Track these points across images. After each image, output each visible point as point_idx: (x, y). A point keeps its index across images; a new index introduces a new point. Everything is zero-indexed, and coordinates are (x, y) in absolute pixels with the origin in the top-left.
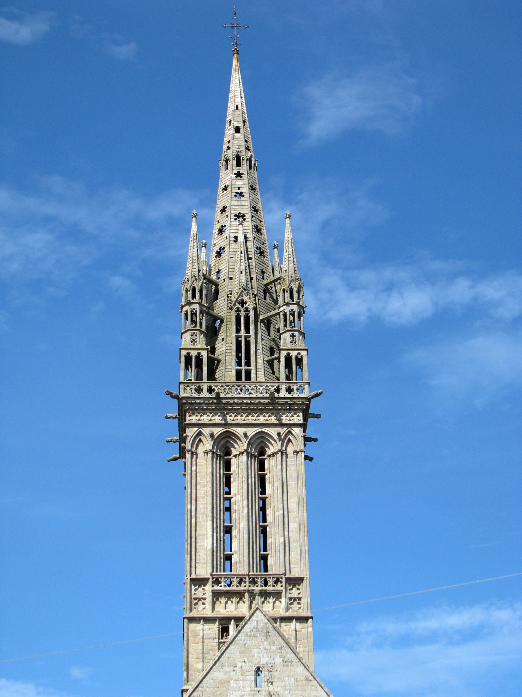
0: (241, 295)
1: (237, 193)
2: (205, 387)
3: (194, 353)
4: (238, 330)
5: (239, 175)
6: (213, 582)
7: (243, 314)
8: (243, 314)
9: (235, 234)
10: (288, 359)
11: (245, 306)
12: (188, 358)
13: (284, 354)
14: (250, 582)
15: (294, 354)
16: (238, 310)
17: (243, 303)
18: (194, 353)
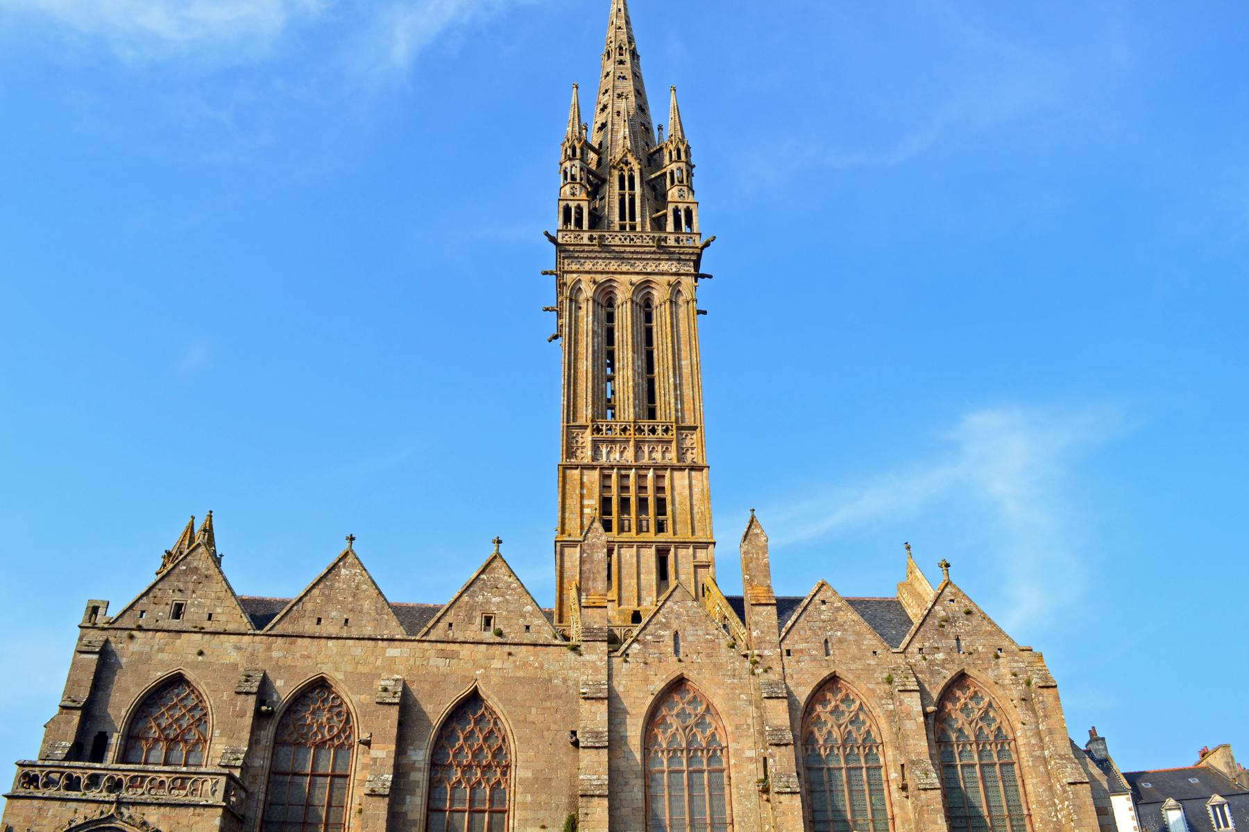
0: (625, 156)
1: (620, 77)
2: (586, 236)
3: (573, 205)
4: (622, 187)
5: (621, 62)
6: (593, 430)
7: (626, 174)
8: (626, 174)
9: (618, 110)
10: (676, 211)
11: (629, 166)
12: (567, 210)
13: (671, 207)
14: (635, 430)
15: (682, 207)
16: (622, 169)
17: (627, 163)
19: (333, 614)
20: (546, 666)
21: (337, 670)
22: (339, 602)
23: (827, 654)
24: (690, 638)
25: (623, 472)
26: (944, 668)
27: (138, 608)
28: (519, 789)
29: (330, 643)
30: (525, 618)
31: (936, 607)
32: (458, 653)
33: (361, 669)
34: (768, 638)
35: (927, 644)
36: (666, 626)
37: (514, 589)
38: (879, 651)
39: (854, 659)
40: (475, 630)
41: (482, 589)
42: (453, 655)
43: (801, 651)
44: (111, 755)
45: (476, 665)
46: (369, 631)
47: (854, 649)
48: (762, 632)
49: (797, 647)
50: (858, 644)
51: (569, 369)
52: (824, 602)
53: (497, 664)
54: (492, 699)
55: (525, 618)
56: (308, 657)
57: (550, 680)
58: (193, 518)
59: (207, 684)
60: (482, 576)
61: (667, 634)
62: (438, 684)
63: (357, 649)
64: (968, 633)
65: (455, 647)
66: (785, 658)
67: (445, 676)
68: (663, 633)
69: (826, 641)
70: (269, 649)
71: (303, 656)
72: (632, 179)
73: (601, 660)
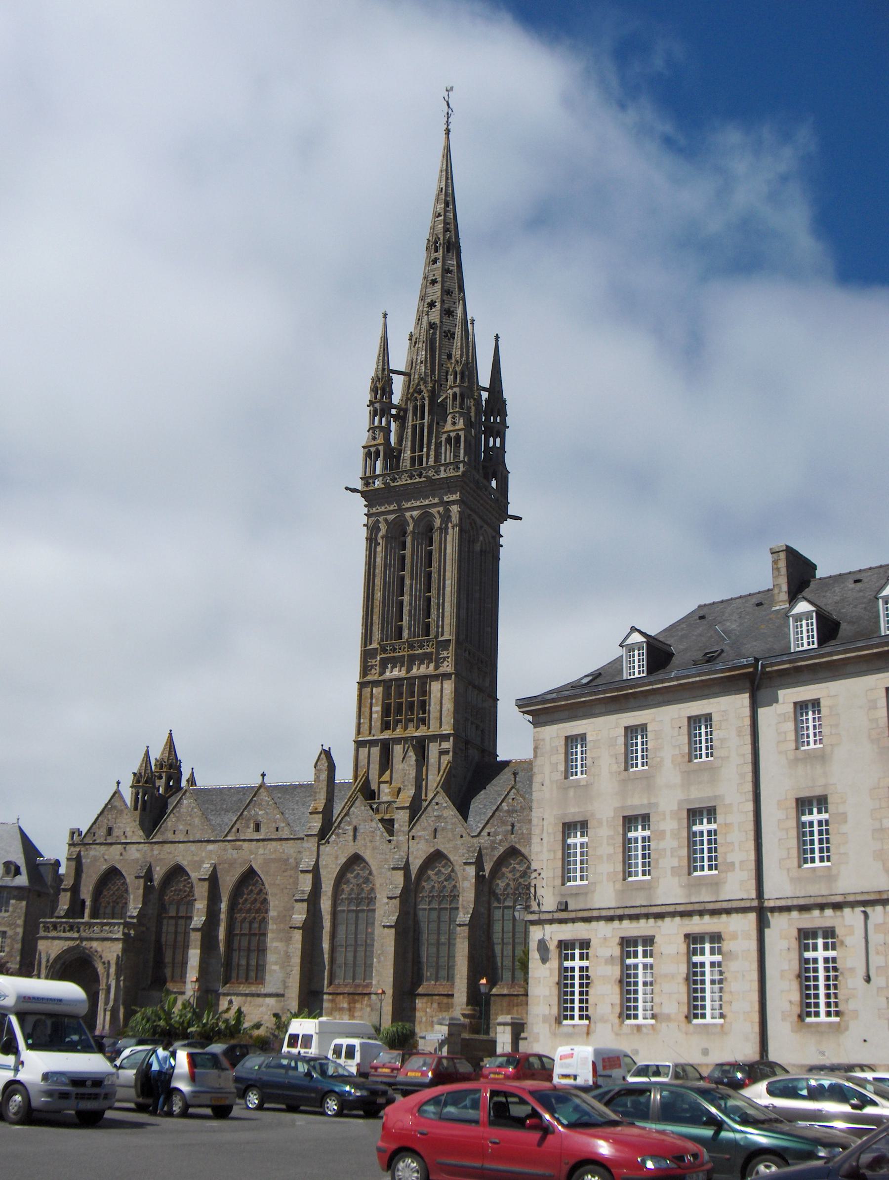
0: (418, 384)
13: (444, 436)
14: (408, 648)
18: (373, 449)
19: (181, 827)
20: (286, 851)
21: (184, 860)
22: (184, 820)
23: (435, 837)
24: (362, 831)
25: (399, 682)
26: (500, 845)
27: (92, 831)
28: (270, 922)
29: (180, 845)
30: (275, 822)
31: (503, 804)
32: (241, 846)
33: (196, 858)
34: (402, 829)
35: (493, 830)
36: (349, 823)
37: (271, 805)
38: (464, 835)
39: (450, 840)
40: (250, 833)
41: (254, 807)
42: (239, 848)
43: (420, 837)
44: (87, 912)
45: (251, 853)
46: (198, 837)
47: (450, 835)
48: (400, 825)
49: (420, 834)
50: (453, 831)
51: (368, 601)
52: (437, 804)
53: (261, 851)
54: (259, 872)
55: (275, 822)
56: (170, 853)
57: (288, 860)
58: (148, 747)
59: (126, 871)
60: (255, 799)
61: (350, 828)
62: (232, 864)
63: (193, 847)
64: (518, 821)
65: (240, 843)
66: (411, 841)
67: (235, 860)
68: (347, 828)
69: (435, 830)
70: (152, 850)
71: (168, 853)
72: (423, 406)
73: (314, 846)
